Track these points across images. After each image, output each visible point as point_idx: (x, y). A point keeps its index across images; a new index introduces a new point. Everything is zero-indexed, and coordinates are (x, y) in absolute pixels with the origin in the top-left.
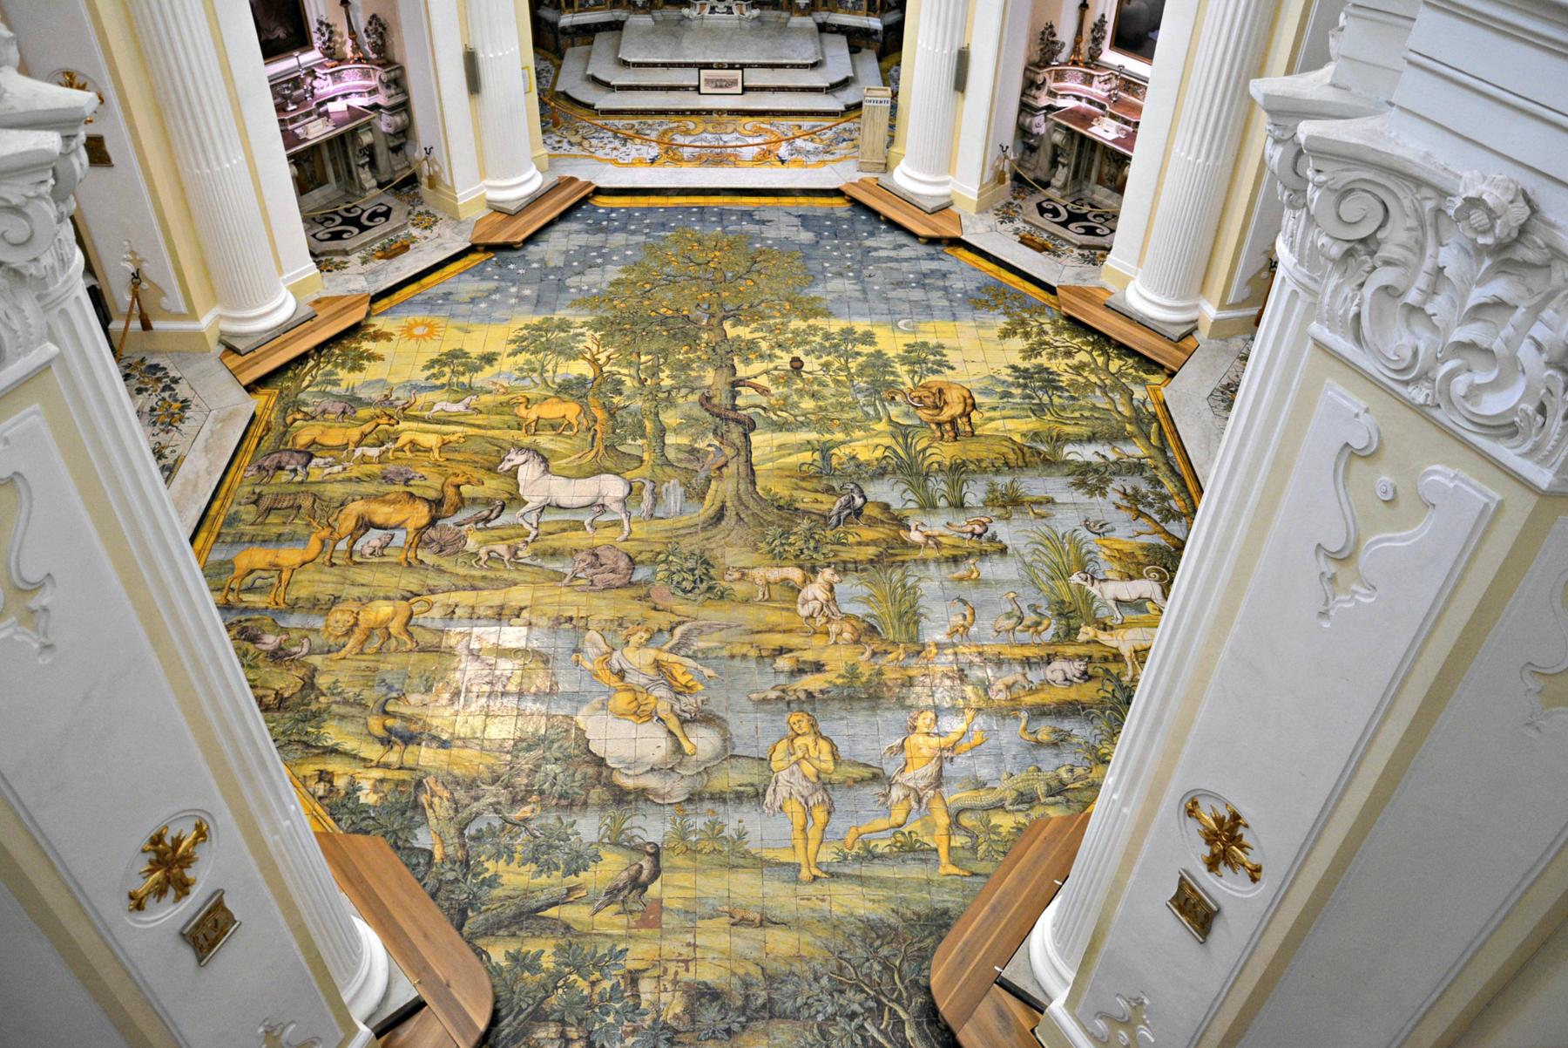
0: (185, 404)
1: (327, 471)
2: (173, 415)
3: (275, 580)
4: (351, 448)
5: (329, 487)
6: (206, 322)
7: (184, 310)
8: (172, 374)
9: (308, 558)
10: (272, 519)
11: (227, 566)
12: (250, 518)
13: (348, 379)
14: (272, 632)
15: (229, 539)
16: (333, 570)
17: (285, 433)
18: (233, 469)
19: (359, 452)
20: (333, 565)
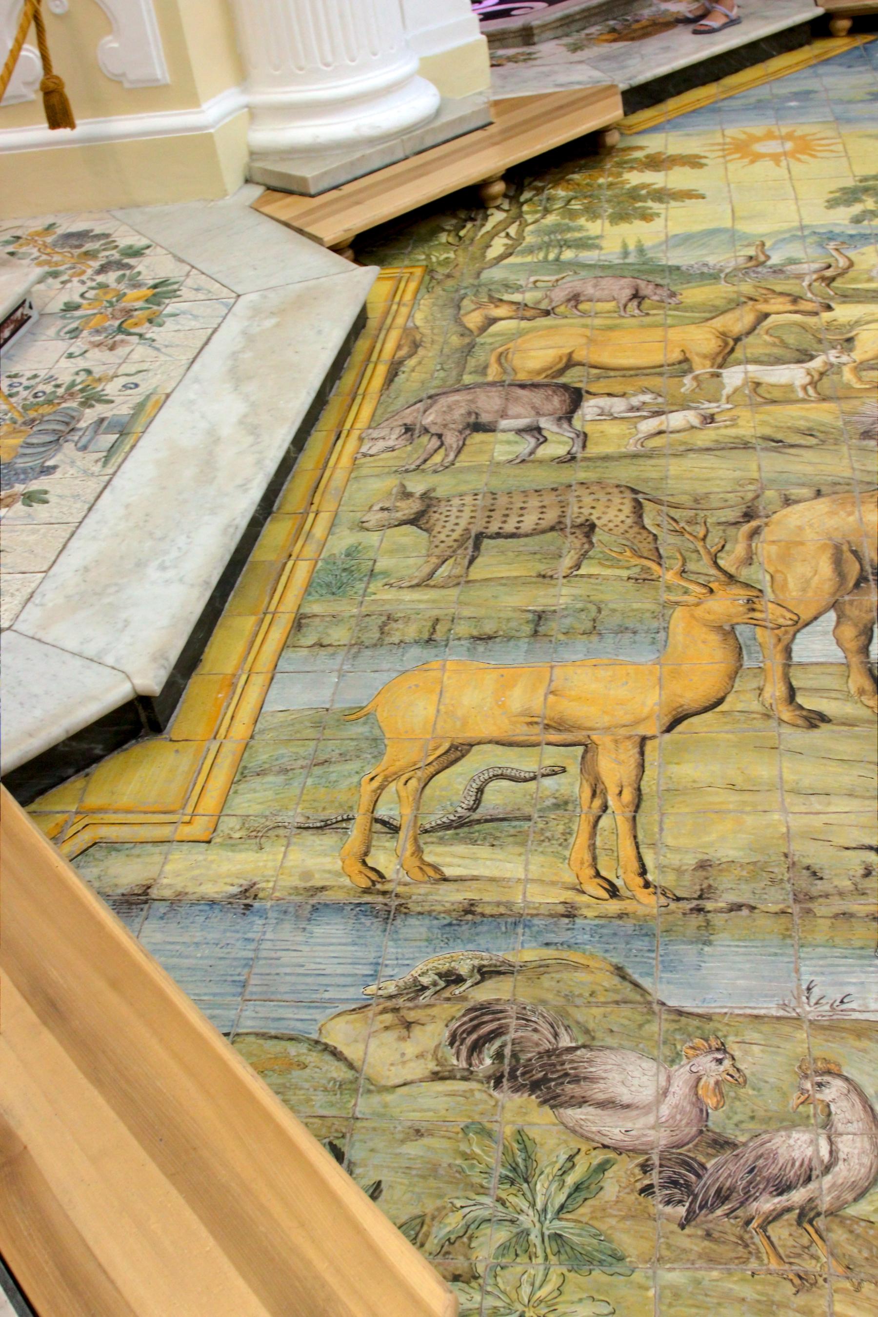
0: (162, 291)
1: (649, 426)
2: (128, 313)
3: (572, 784)
4: (702, 368)
5: (675, 467)
6: (215, 108)
7: (160, 71)
8: (123, 242)
9: (692, 693)
10: (492, 563)
11: (348, 730)
12: (414, 565)
13: (615, 239)
14: (634, 1041)
15: (340, 635)
16: (821, 736)
17: (470, 348)
18: (318, 440)
19: (734, 377)
20: (816, 720)
